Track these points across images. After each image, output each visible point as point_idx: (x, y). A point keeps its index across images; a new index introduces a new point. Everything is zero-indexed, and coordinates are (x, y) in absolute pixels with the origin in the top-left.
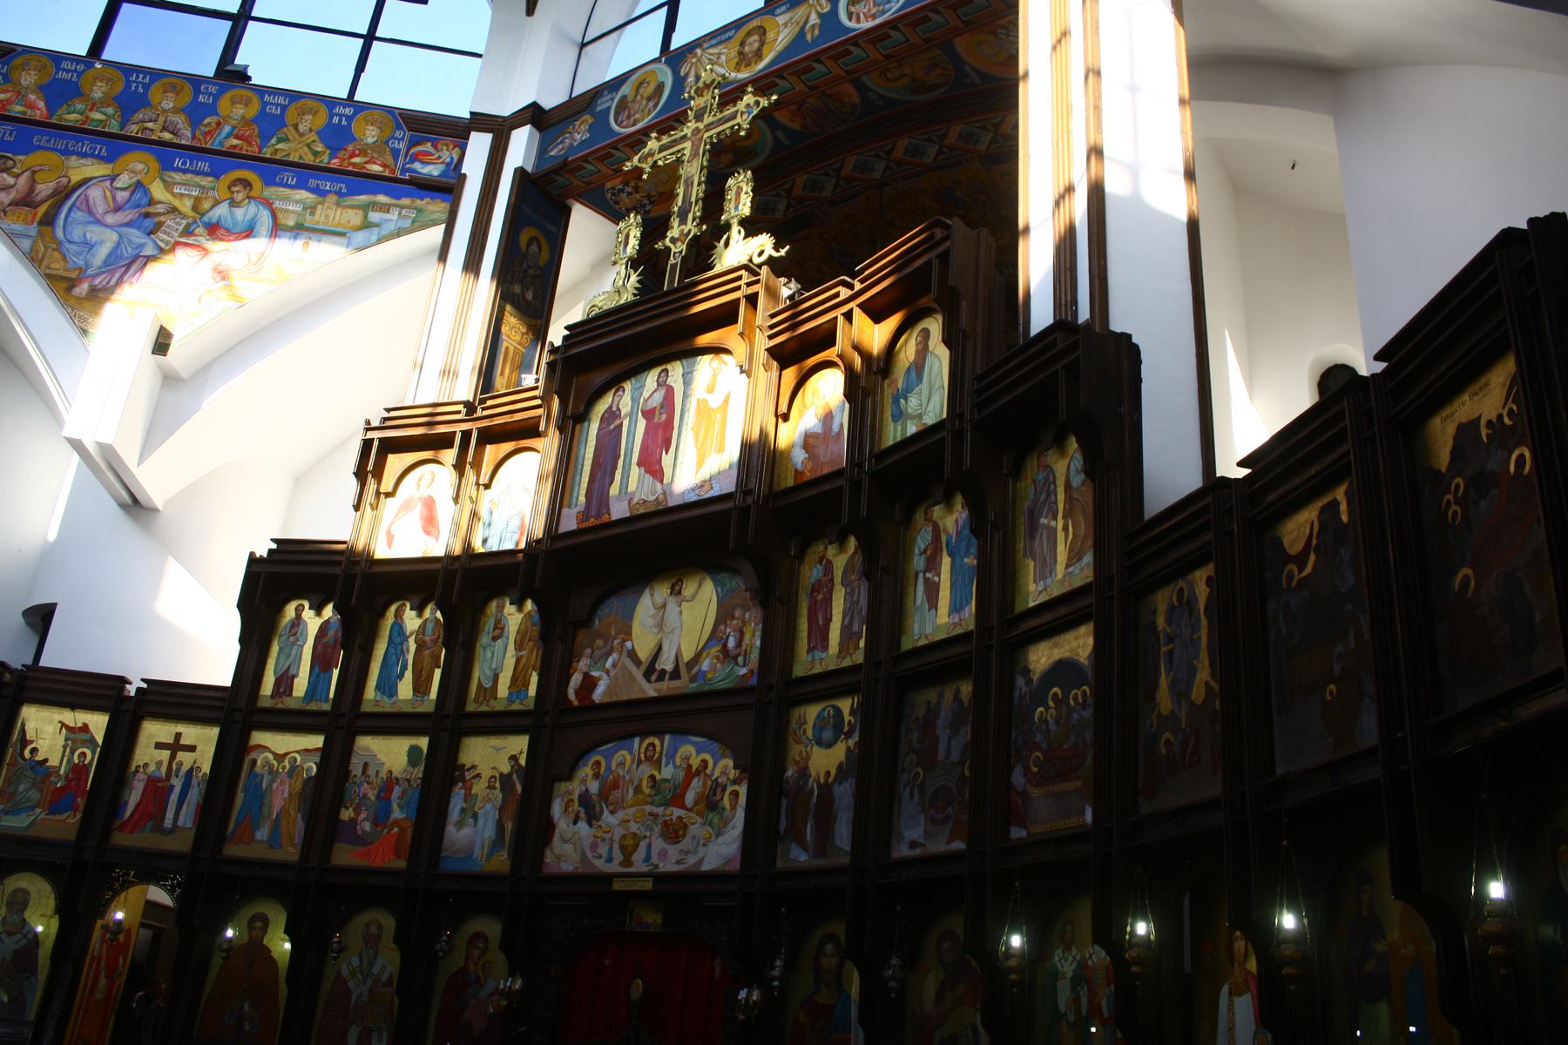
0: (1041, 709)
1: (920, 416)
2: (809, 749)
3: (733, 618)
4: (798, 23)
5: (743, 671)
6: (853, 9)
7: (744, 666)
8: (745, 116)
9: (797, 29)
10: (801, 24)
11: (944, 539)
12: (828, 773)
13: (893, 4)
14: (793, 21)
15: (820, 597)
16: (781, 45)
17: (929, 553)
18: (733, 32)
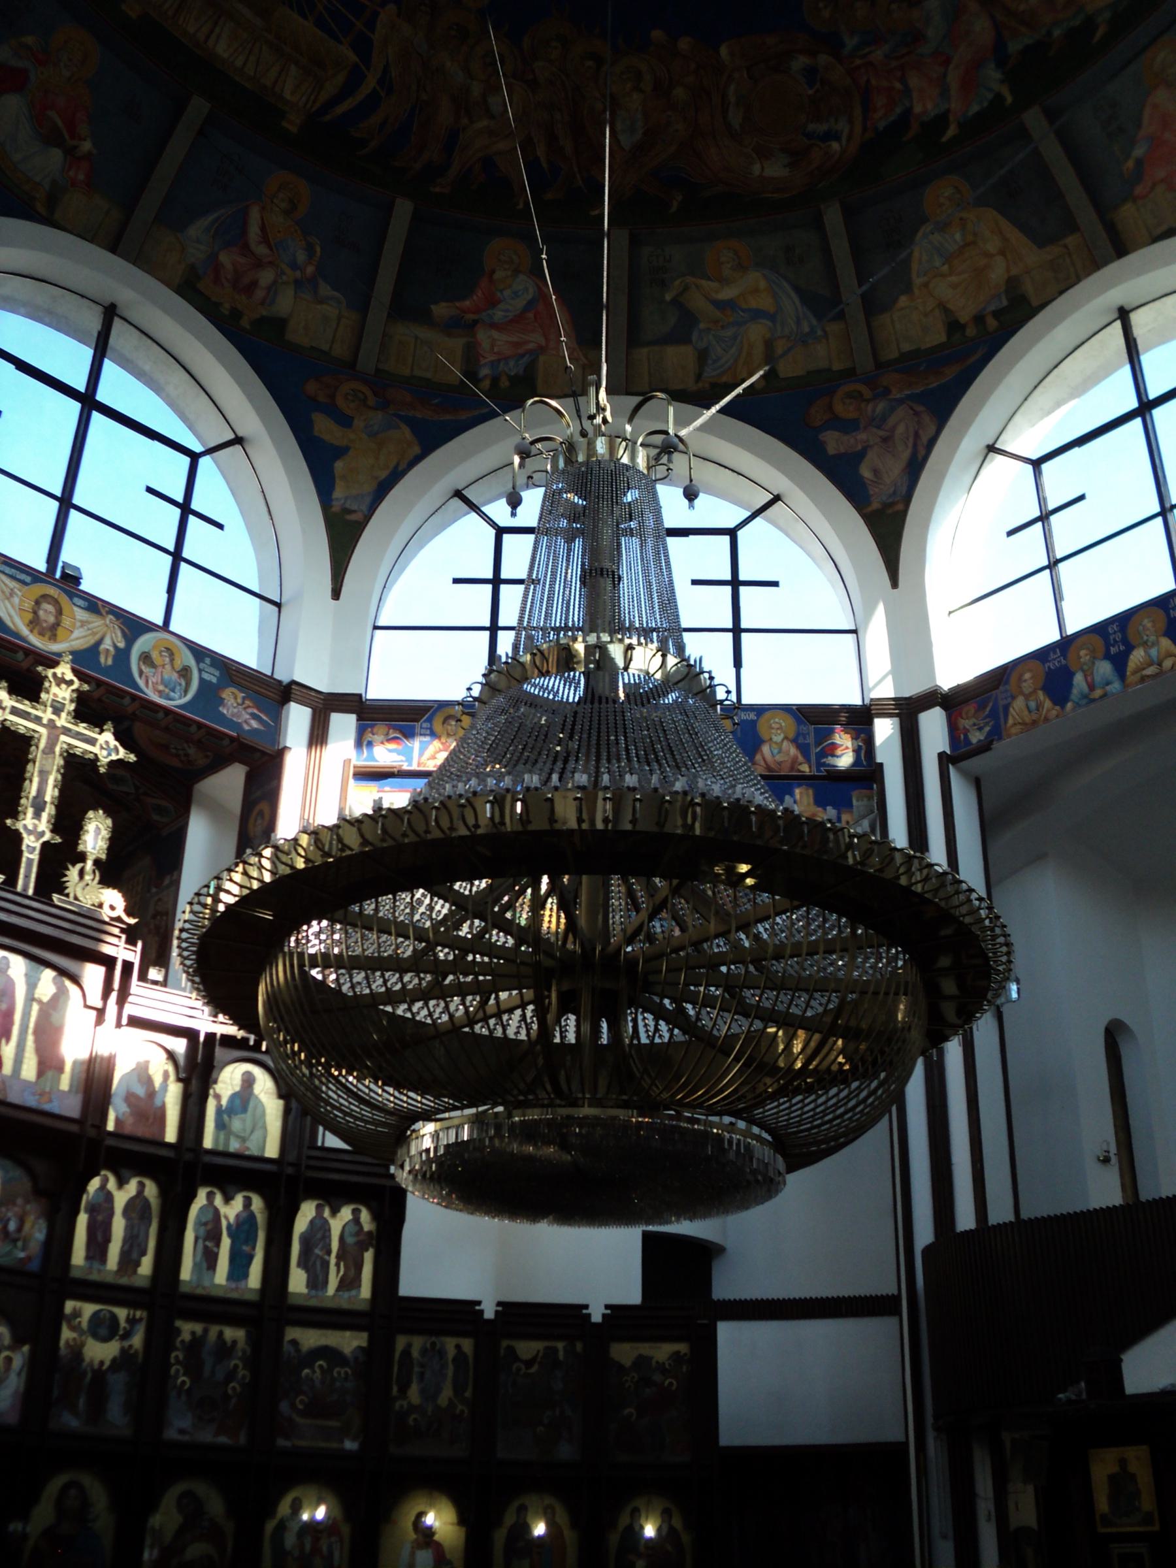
0: (306, 1371)
1: (243, 1140)
2: (83, 1338)
3: (14, 1204)
4: (94, 634)
5: (22, 1255)
6: (143, 668)
7: (24, 1249)
8: (105, 753)
9: (91, 641)
10: (97, 637)
11: (224, 1223)
12: (102, 1363)
13: (176, 696)
14: (91, 626)
15: (100, 1218)
16: (78, 642)
17: (209, 1227)
18: (28, 579)
